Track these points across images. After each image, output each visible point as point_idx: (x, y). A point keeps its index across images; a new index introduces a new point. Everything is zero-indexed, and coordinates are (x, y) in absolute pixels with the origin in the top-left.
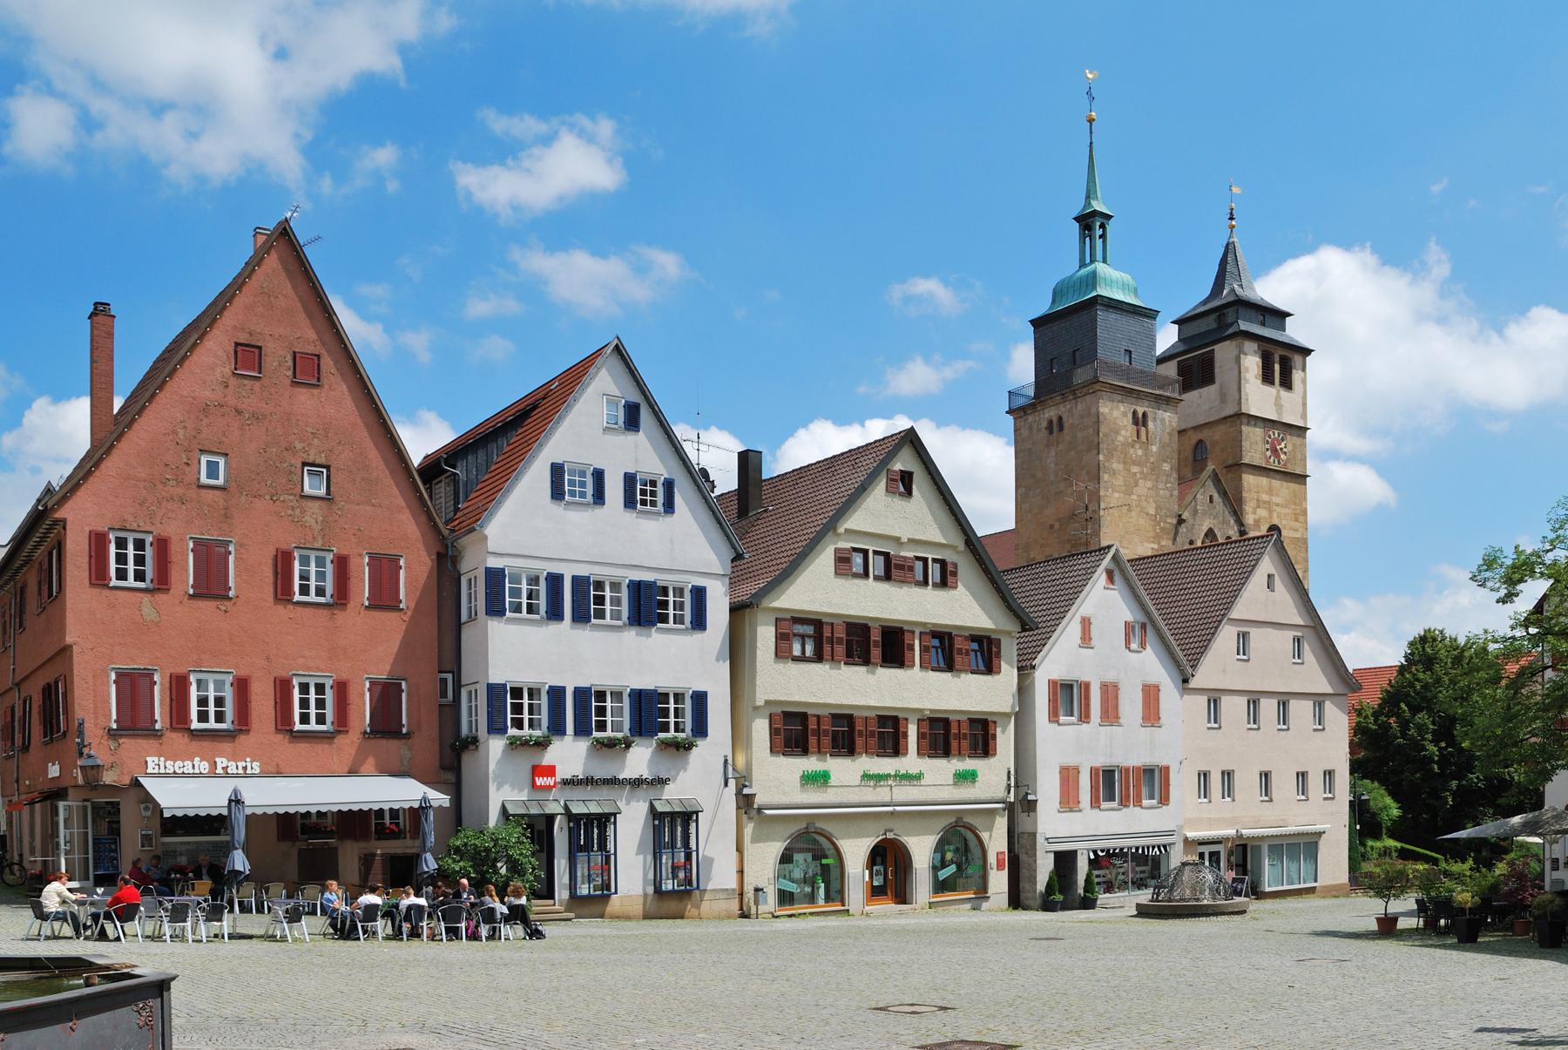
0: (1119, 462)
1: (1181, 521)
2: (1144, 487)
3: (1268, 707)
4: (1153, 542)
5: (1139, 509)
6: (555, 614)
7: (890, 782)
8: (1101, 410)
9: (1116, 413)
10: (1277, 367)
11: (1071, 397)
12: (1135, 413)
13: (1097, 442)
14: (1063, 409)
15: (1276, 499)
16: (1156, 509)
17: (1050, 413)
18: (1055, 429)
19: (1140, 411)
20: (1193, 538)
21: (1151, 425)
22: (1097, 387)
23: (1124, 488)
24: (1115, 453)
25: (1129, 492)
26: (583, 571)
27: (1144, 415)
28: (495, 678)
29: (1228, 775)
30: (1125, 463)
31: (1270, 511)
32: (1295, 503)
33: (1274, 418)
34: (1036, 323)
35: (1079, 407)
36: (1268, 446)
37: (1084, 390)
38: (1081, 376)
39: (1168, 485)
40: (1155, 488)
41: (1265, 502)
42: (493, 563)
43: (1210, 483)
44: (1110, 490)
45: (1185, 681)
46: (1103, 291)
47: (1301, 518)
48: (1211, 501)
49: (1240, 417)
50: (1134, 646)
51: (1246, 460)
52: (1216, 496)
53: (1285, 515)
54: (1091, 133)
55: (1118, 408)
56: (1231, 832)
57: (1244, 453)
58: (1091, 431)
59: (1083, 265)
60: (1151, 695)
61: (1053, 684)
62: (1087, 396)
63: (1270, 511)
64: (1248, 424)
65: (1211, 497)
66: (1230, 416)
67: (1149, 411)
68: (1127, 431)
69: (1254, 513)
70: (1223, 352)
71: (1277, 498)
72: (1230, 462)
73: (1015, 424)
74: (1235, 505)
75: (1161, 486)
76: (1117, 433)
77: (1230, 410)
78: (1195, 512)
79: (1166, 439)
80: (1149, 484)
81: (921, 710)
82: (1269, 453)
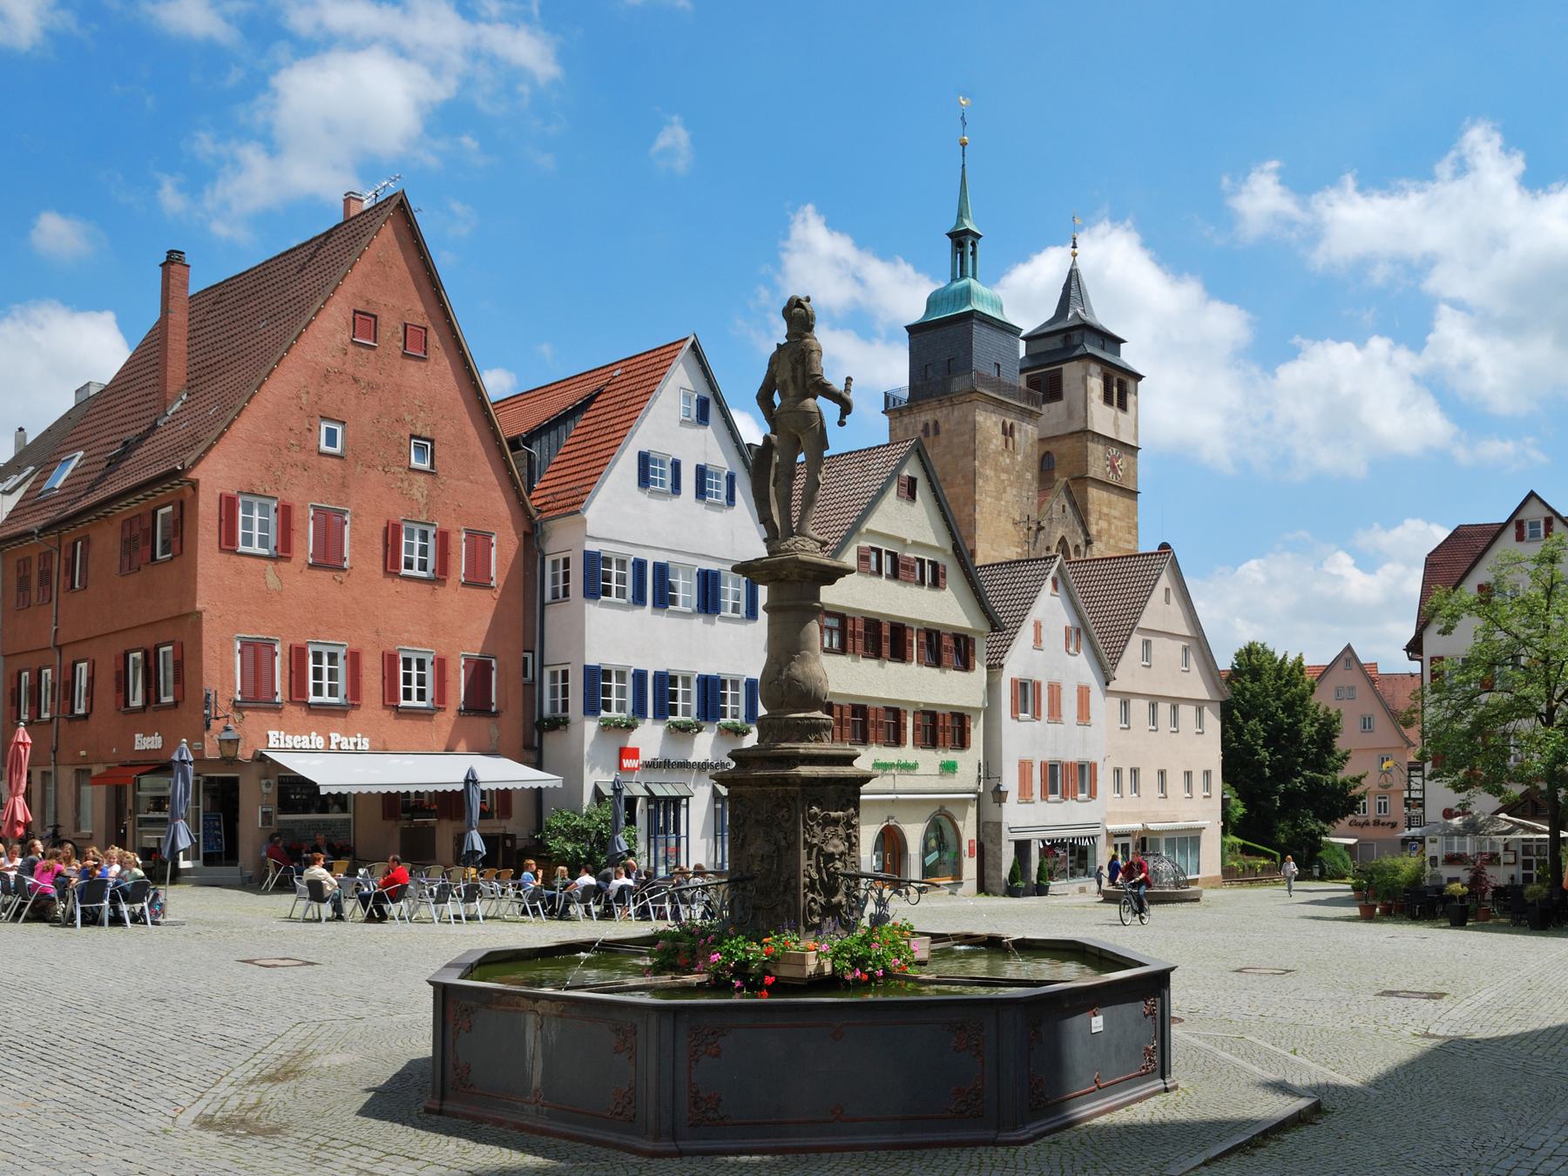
1: (1040, 529)
2: (1011, 494)
3: (1164, 709)
4: (1017, 547)
6: (639, 599)
7: (893, 771)
8: (977, 418)
9: (989, 423)
10: (1115, 390)
11: (948, 404)
12: (1004, 423)
13: (972, 448)
14: (940, 415)
15: (1115, 513)
17: (927, 417)
18: (931, 432)
19: (1009, 421)
21: (1017, 435)
22: (974, 396)
23: (994, 494)
25: (998, 499)
26: (662, 558)
27: (1012, 426)
28: (592, 660)
29: (1135, 772)
30: (996, 470)
31: (1110, 523)
32: (1129, 518)
33: (1113, 436)
34: (913, 330)
35: (956, 413)
36: (1108, 463)
37: (961, 399)
38: (958, 384)
40: (1020, 495)
41: (1105, 515)
42: (591, 546)
43: (1062, 494)
45: (1107, 684)
46: (976, 305)
47: (1133, 531)
48: (1064, 511)
49: (1086, 434)
50: (1071, 650)
51: (1091, 474)
52: (1067, 505)
54: (964, 155)
55: (991, 418)
56: (1137, 826)
58: (967, 437)
59: (954, 279)
60: (1083, 693)
61: (1014, 681)
62: (965, 405)
63: (1110, 523)
64: (1092, 441)
65: (1064, 506)
66: (1077, 432)
67: (1015, 422)
68: (997, 441)
69: (1097, 524)
70: (1071, 371)
72: (1076, 475)
73: (890, 424)
74: (1081, 514)
75: (1024, 494)
76: (990, 441)
77: (1076, 427)
78: (1051, 520)
79: (1029, 450)
80: (1014, 492)
81: (917, 703)
82: (1108, 469)
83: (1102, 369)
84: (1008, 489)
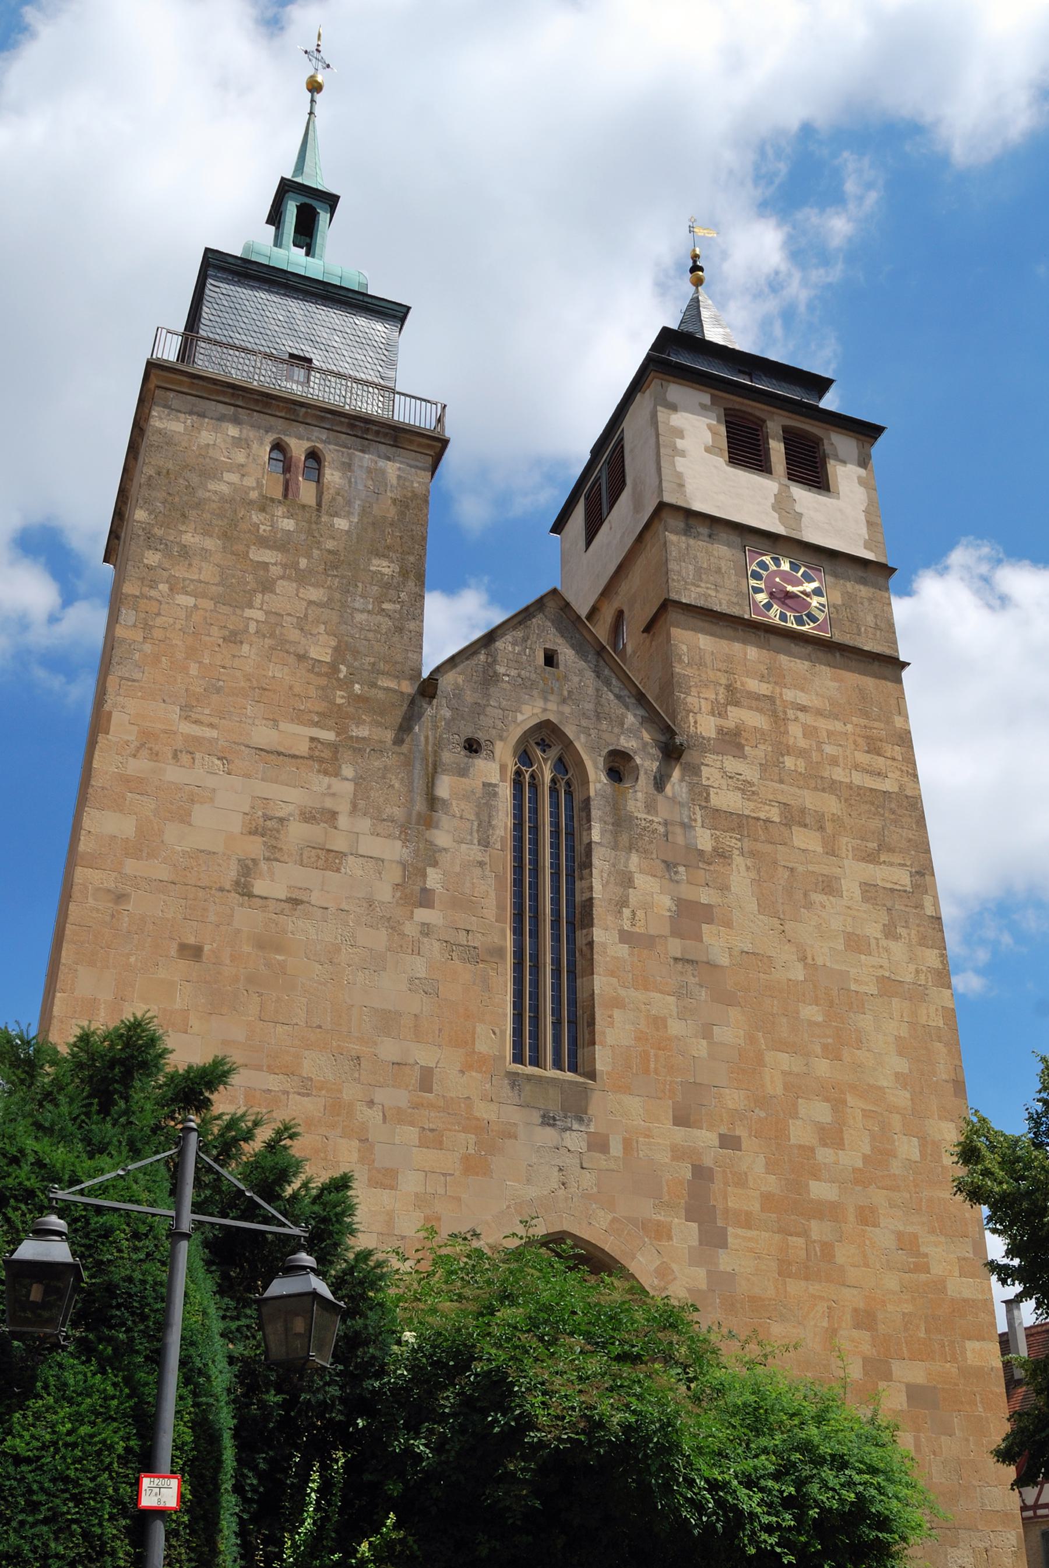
0: (207, 533)
5: (268, 642)
16: (336, 649)
20: (480, 736)
24: (193, 514)
30: (225, 536)
31: (779, 720)
33: (780, 529)
39: (386, 606)
44: (163, 587)
53: (830, 734)
57: (671, 584)
64: (687, 532)
71: (800, 694)
83: (713, 396)
84: (282, 586)
